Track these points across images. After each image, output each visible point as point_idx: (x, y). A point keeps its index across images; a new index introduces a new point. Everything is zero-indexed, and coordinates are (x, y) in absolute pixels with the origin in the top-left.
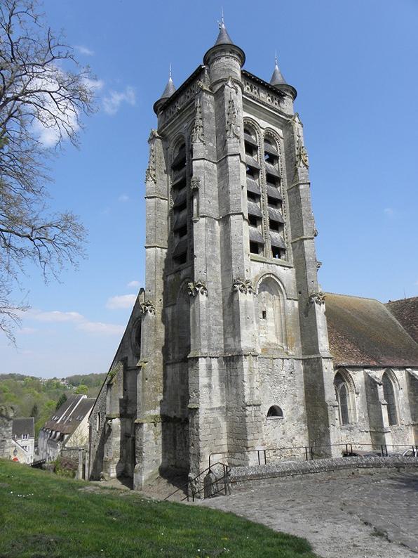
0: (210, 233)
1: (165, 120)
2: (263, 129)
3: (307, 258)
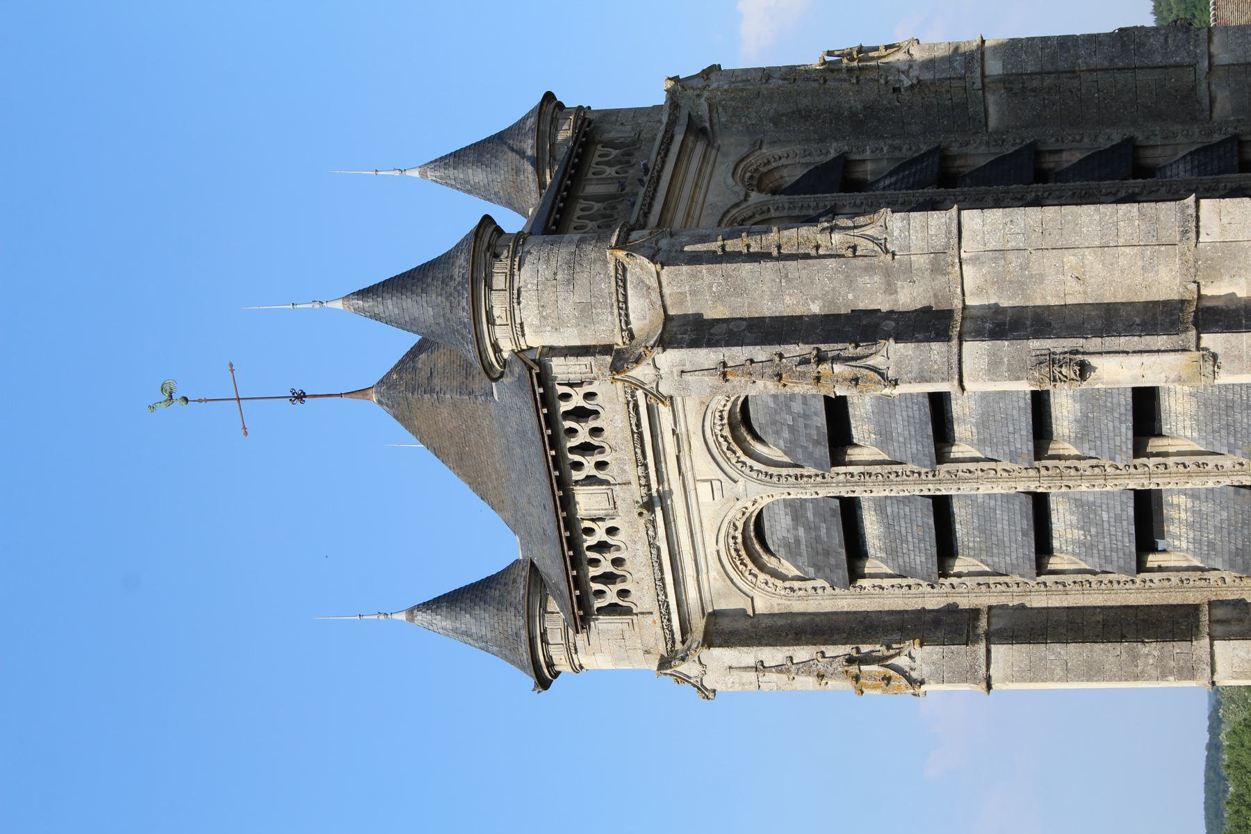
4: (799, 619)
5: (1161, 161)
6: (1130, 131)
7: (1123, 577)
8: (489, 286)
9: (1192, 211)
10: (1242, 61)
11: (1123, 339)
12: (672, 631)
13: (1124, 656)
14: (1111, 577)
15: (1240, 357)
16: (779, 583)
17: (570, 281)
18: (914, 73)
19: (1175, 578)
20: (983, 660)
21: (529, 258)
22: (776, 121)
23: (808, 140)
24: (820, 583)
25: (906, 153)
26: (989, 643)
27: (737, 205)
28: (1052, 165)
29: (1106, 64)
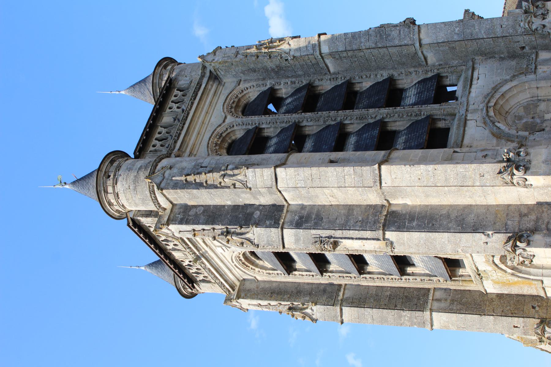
0: (415, 224)
1: (209, 282)
2: (226, 117)
3: (456, 38)
4: (274, 284)
5: (406, 86)
6: (391, 72)
7: (397, 277)
8: (106, 192)
9: (377, 172)
10: (435, 42)
11: (351, 232)
12: (227, 288)
13: (396, 316)
14: (392, 277)
15: (404, 244)
16: (264, 271)
17: (135, 189)
18: (292, 53)
19: (419, 279)
20: (339, 314)
21: (120, 179)
22: (243, 72)
23: (259, 79)
24: (279, 272)
25: (298, 86)
26: (341, 305)
27: (220, 125)
28: (358, 89)
29: (374, 46)
